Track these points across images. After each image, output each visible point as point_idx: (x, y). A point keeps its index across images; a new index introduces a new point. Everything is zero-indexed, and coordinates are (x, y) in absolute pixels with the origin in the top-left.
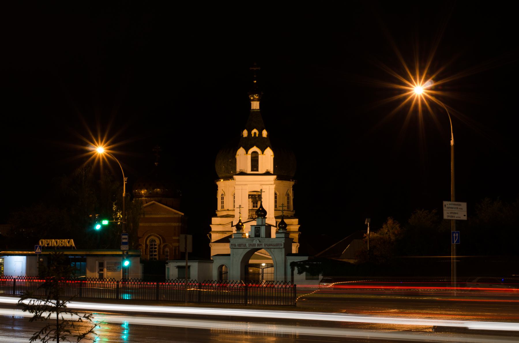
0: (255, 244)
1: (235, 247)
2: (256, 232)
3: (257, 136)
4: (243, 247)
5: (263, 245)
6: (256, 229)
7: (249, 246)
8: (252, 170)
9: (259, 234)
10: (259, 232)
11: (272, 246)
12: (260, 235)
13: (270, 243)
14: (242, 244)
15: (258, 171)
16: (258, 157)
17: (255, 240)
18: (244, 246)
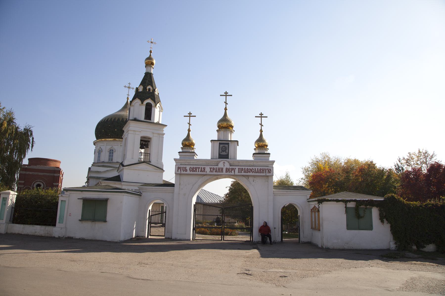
0: (222, 169)
1: (185, 172)
2: (221, 151)
3: (151, 91)
4: (200, 173)
5: (237, 171)
6: (221, 145)
7: (211, 171)
9: (226, 154)
10: (227, 151)
12: (228, 155)
13: (249, 168)
14: (199, 168)
15: (150, 119)
17: (223, 162)
18: (201, 171)
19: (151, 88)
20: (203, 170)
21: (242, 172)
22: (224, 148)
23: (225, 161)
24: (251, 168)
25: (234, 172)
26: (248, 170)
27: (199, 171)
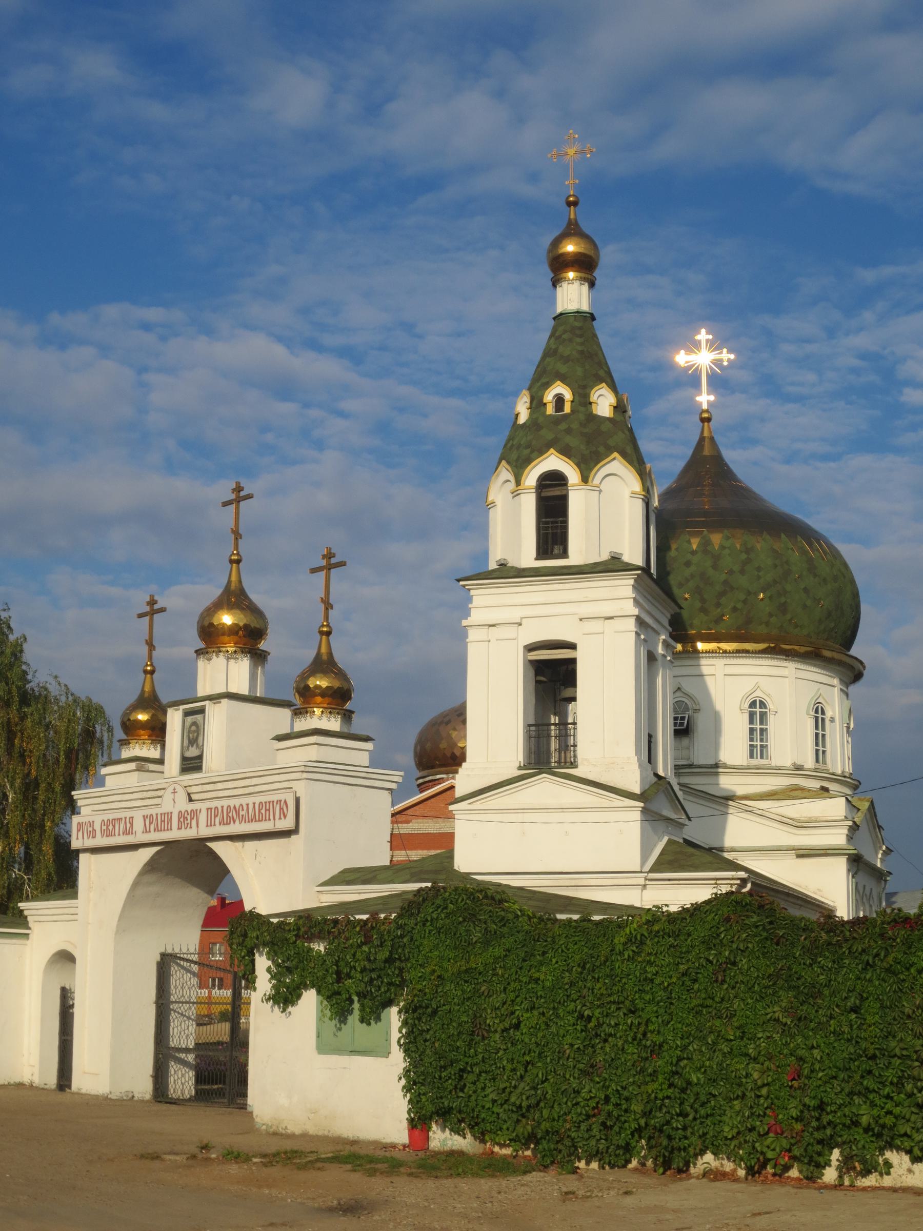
3: (567, 409)
5: (203, 818)
6: (190, 719)
7: (146, 831)
8: (537, 559)
11: (243, 819)
12: (200, 757)
14: (120, 819)
15: (564, 554)
16: (564, 499)
18: (126, 833)
19: (568, 395)
20: (128, 825)
21: (215, 825)
22: (194, 728)
23: (179, 789)
24: (236, 802)
25: (198, 826)
26: (230, 815)
27: (119, 835)
